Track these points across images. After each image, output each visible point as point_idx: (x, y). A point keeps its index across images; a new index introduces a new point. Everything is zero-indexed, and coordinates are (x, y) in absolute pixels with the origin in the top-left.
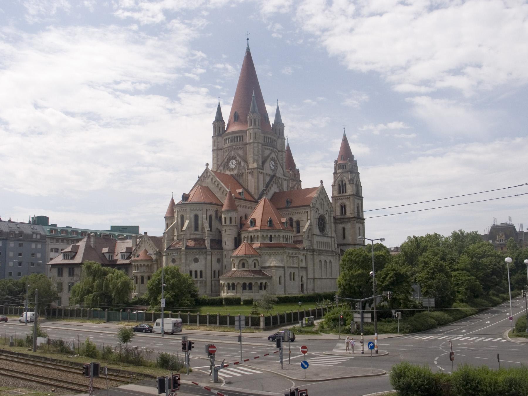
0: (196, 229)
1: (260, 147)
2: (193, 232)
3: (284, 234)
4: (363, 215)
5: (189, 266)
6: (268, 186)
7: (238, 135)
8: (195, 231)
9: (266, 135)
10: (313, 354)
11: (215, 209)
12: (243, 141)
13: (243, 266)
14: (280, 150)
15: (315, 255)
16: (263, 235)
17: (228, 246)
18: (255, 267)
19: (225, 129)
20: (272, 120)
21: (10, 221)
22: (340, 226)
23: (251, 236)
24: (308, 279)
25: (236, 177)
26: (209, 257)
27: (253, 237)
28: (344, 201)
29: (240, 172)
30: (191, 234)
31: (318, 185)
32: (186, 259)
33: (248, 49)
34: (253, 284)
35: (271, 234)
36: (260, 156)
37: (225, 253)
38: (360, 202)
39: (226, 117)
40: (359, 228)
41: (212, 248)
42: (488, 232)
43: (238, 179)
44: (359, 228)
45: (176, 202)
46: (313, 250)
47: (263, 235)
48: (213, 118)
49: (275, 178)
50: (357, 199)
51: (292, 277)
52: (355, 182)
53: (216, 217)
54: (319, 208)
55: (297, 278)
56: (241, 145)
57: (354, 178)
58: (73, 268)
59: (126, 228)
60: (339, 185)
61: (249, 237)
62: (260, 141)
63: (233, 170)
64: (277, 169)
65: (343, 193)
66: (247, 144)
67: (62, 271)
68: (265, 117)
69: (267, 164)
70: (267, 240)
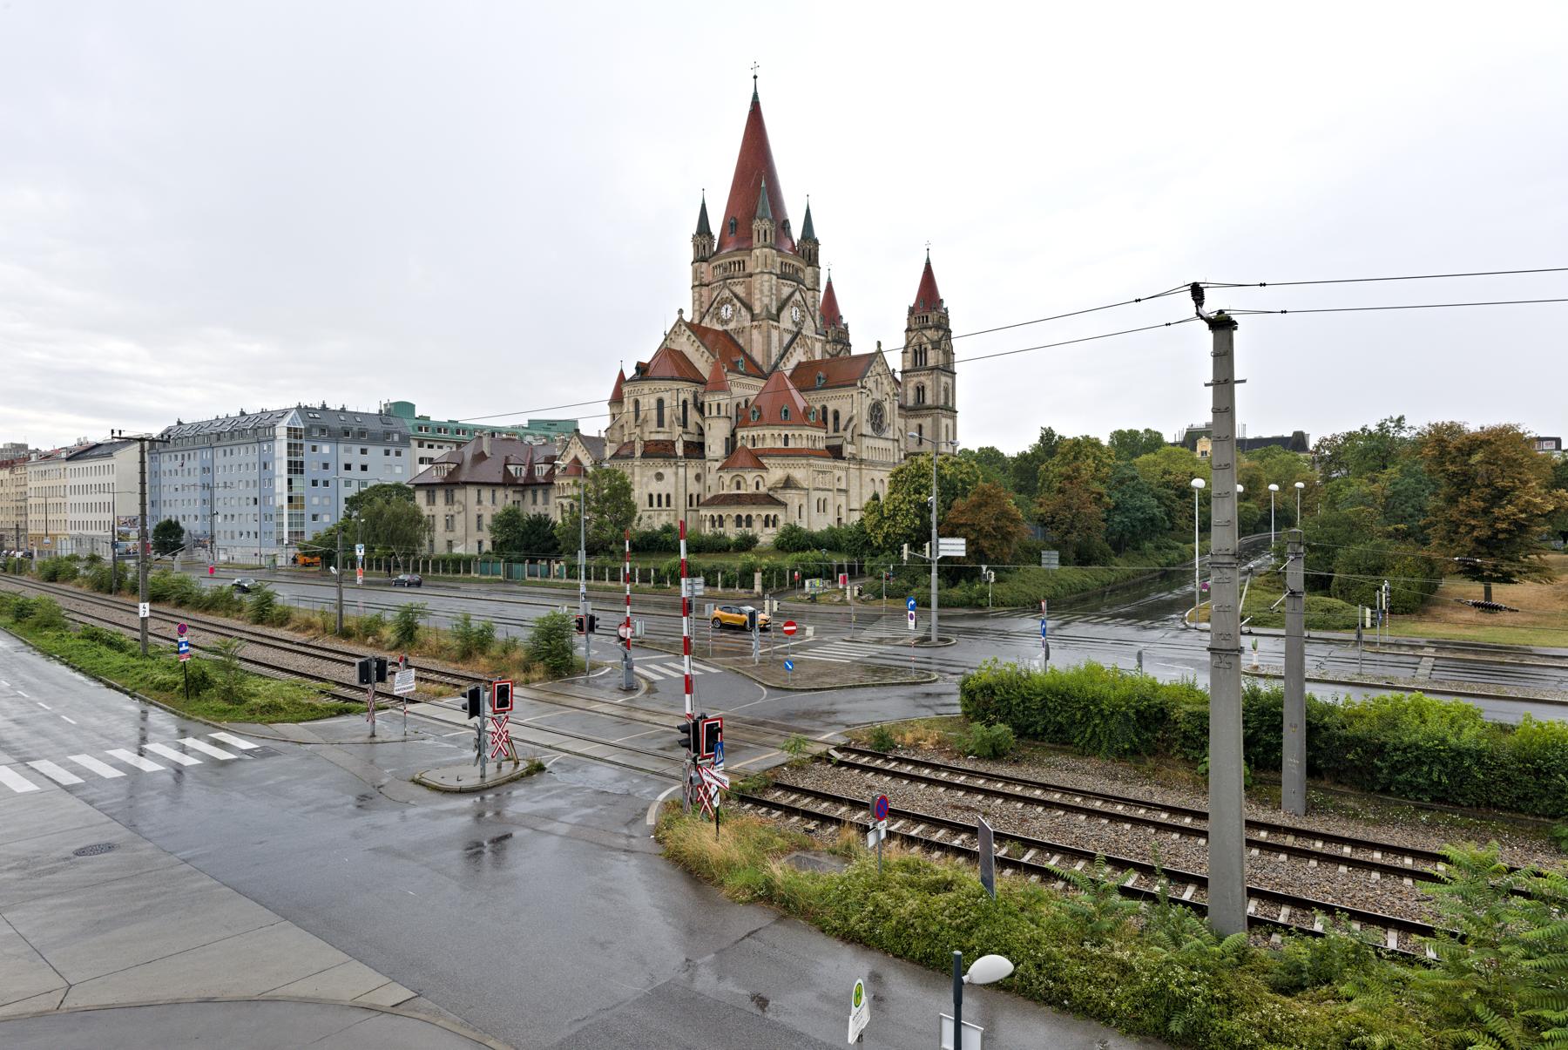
0: (660, 423)
1: (774, 282)
3: (809, 433)
4: (954, 404)
5: (647, 486)
6: (785, 351)
7: (736, 259)
8: (659, 426)
9: (786, 260)
10: (825, 639)
11: (693, 389)
13: (738, 488)
14: (809, 286)
15: (864, 472)
17: (714, 452)
18: (757, 488)
19: (715, 249)
20: (796, 232)
21: (343, 410)
22: (914, 422)
24: (851, 510)
26: (681, 471)
28: (922, 379)
30: (651, 432)
31: (873, 349)
32: (642, 475)
33: (755, 96)
34: (754, 517)
35: (787, 432)
36: (774, 297)
37: (708, 464)
38: (950, 381)
39: (716, 227)
40: (947, 426)
41: (687, 456)
42: (1180, 439)
43: (736, 337)
44: (947, 426)
45: (628, 376)
46: (861, 461)
48: (694, 229)
49: (800, 336)
50: (945, 375)
51: (822, 506)
52: (943, 346)
53: (695, 405)
54: (874, 389)
55: (831, 510)
62: (774, 271)
63: (726, 322)
64: (803, 322)
66: (751, 275)
67: (434, 496)
68: (784, 226)
69: (785, 314)
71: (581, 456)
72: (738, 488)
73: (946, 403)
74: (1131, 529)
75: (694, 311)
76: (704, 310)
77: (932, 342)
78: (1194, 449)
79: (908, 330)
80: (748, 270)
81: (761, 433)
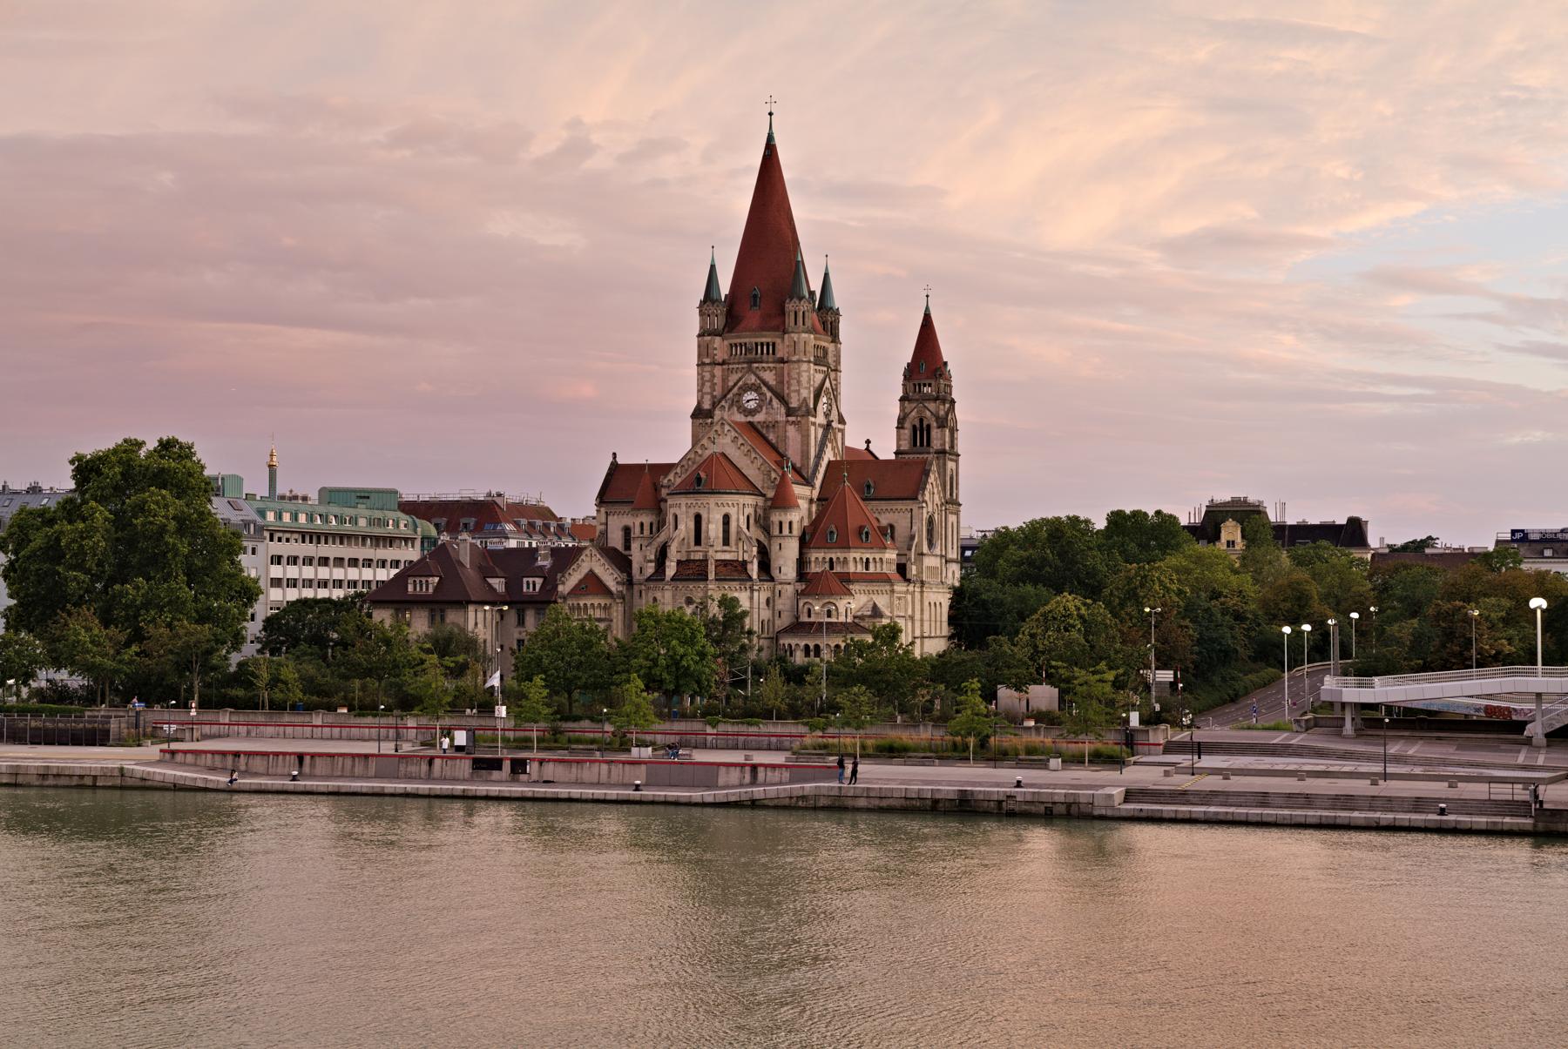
0: (726, 541)
2: (719, 545)
9: (818, 343)
12: (774, 353)
13: (829, 614)
16: (855, 558)
17: (786, 575)
23: (831, 559)
25: (759, 427)
26: (756, 594)
27: (834, 560)
29: (770, 419)
33: (770, 138)
35: (868, 556)
42: (1197, 519)
43: (764, 432)
47: (855, 558)
56: (773, 362)
57: (947, 414)
58: (442, 611)
59: (366, 495)
60: (914, 427)
61: (827, 560)
65: (922, 444)
70: (859, 566)
71: (599, 571)
72: (829, 614)
73: (951, 494)
74: (1208, 660)
75: (698, 391)
76: (718, 393)
77: (937, 418)
78: (1216, 537)
79: (902, 400)
80: (779, 355)
81: (841, 555)
